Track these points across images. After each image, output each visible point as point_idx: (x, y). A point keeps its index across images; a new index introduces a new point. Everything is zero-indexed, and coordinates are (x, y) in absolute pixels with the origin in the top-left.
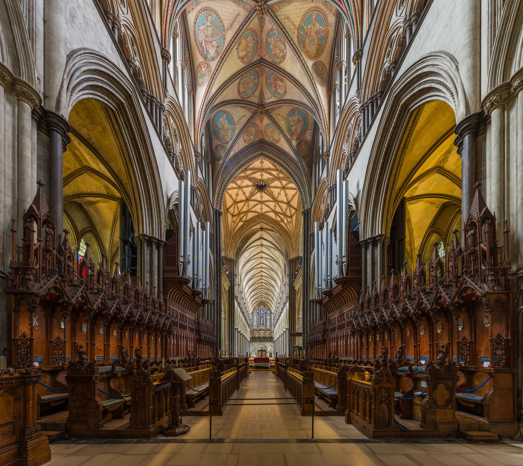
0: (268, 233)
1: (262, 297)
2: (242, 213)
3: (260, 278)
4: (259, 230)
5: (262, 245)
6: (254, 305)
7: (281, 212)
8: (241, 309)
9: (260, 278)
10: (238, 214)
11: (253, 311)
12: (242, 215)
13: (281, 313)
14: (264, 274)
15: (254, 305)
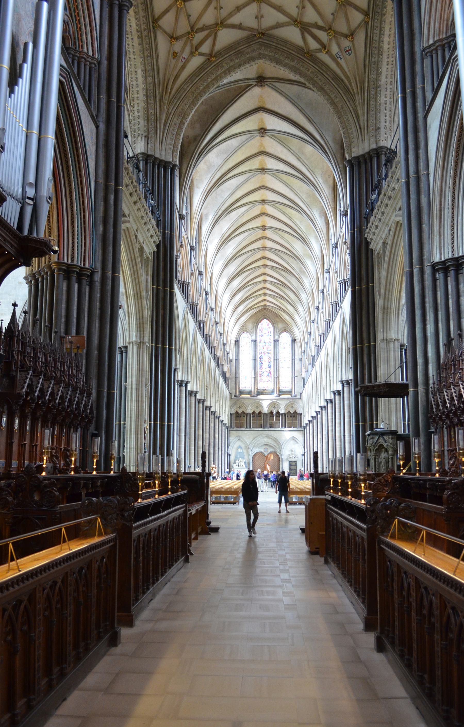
0: (281, 93)
1: (265, 294)
2: (202, 29)
3: (260, 233)
4: (251, 82)
5: (262, 131)
6: (243, 319)
7: (321, 23)
8: (200, 325)
9: (260, 233)
10: (189, 33)
11: (239, 335)
12: (199, 36)
13: (324, 337)
14: (270, 222)
15: (243, 319)
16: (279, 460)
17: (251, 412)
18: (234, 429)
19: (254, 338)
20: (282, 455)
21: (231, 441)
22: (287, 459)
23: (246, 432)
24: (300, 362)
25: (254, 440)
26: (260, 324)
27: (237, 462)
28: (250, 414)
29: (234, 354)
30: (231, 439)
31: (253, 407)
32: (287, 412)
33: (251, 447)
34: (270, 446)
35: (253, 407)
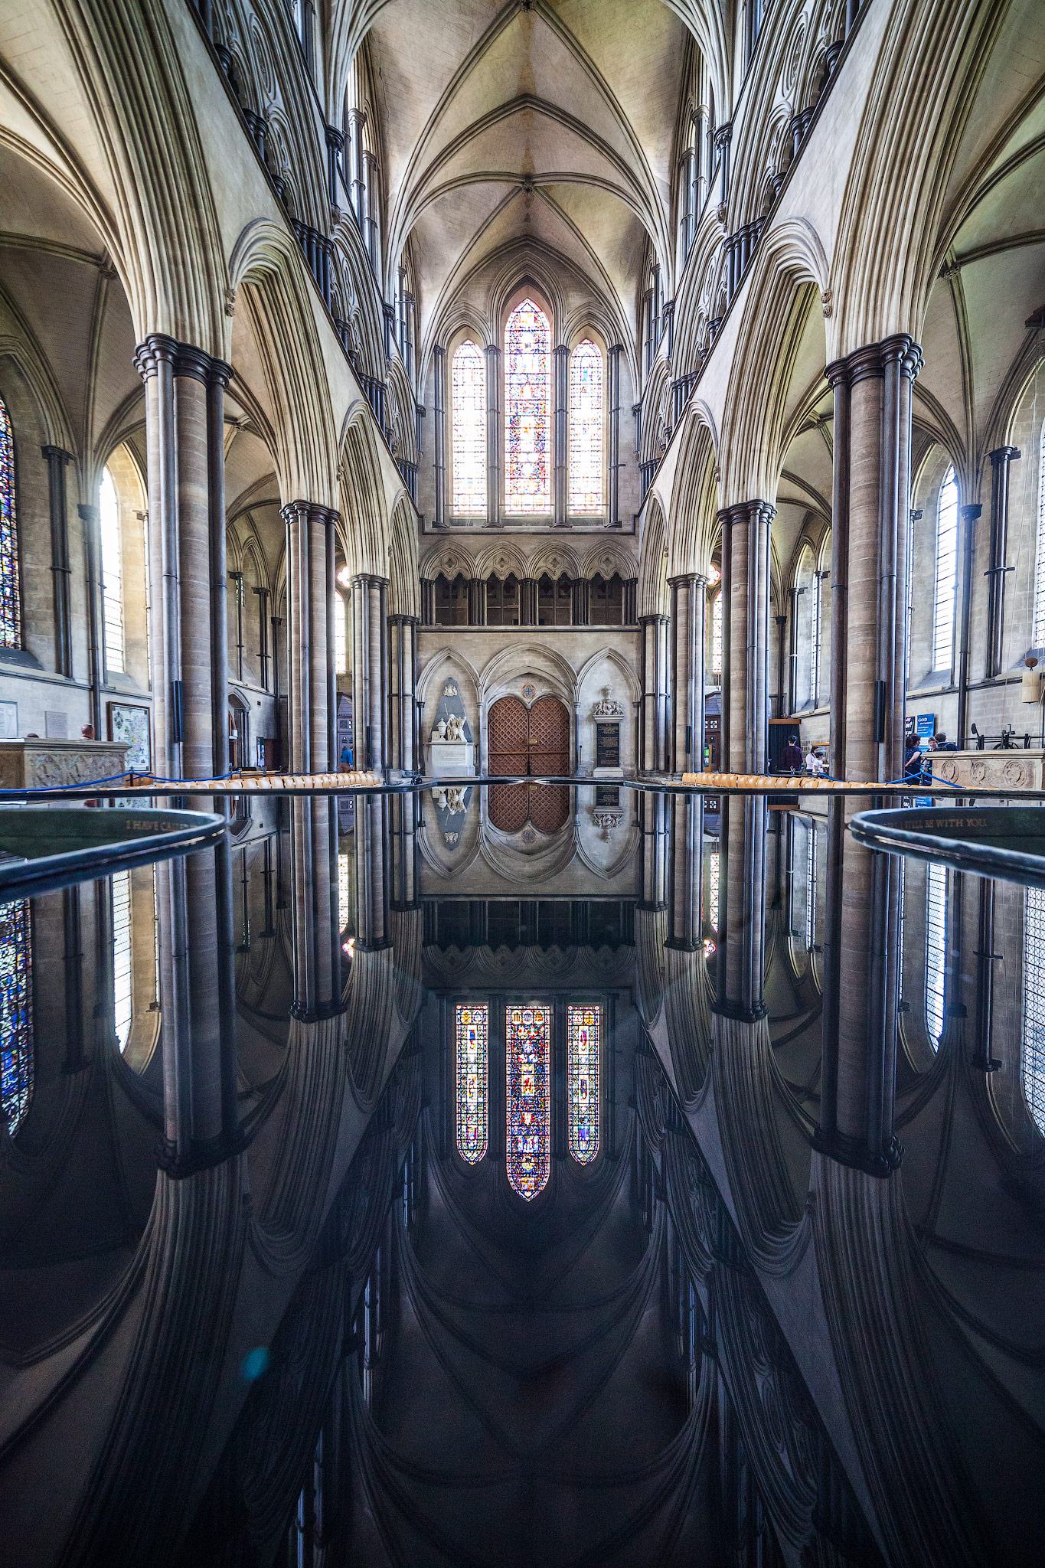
16: (568, 721)
17: (485, 576)
18: (434, 627)
19: (491, 339)
20: (575, 706)
21: (423, 662)
22: (591, 718)
23: (468, 636)
24: (632, 420)
25: (493, 661)
26: (513, 315)
27: (443, 726)
28: (480, 582)
29: (432, 392)
30: (423, 656)
31: (490, 563)
32: (590, 576)
33: (484, 680)
34: (541, 679)
35: (490, 563)
